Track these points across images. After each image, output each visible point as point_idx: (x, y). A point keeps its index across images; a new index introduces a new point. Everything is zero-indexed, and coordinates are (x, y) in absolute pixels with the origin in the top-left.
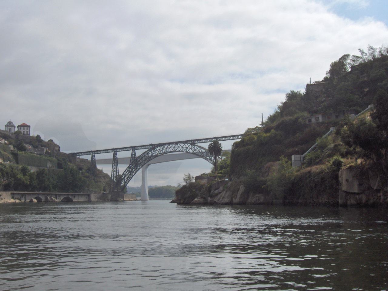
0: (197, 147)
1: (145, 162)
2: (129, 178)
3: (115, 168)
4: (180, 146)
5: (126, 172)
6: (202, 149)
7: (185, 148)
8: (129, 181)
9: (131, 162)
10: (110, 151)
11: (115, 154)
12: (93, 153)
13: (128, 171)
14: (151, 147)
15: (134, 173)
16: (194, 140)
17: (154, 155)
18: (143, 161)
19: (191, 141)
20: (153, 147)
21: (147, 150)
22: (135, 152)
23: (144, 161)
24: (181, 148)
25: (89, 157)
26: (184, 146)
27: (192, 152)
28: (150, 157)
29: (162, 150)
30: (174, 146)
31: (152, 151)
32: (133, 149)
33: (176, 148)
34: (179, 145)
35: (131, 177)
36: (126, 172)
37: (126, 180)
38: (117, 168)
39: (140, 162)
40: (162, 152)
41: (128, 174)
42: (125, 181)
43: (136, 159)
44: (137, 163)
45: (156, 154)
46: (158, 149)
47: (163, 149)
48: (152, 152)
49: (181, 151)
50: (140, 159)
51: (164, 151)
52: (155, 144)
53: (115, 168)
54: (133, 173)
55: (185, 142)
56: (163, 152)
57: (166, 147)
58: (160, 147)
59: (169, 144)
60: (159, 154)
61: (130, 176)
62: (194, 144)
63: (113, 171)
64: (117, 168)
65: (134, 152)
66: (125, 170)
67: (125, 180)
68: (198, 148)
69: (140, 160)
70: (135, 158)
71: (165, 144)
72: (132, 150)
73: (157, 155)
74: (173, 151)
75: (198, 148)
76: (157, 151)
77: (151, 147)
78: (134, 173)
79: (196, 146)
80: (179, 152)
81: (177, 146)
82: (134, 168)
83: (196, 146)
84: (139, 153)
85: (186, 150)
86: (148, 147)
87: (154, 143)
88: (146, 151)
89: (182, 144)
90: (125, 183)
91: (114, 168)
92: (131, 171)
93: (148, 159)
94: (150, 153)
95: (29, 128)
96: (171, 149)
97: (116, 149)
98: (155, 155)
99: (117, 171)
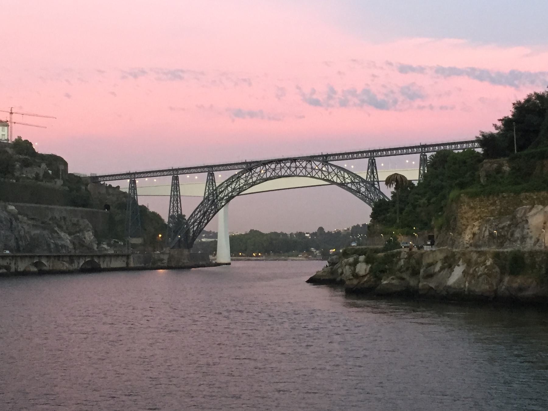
0: (334, 168)
3: (175, 205)
4: (301, 166)
5: (196, 212)
6: (342, 172)
7: (309, 170)
9: (207, 193)
10: (166, 173)
11: (176, 179)
12: (132, 176)
13: (200, 211)
14: (244, 166)
15: (211, 215)
16: (327, 156)
17: (251, 181)
18: (228, 193)
19: (322, 156)
20: (249, 167)
21: (236, 172)
22: (212, 175)
23: (232, 192)
24: (301, 169)
25: (124, 185)
26: (309, 166)
27: (323, 177)
28: (243, 186)
29: (266, 172)
30: (288, 164)
31: (247, 174)
32: (211, 170)
33: (293, 169)
34: (297, 163)
35: (206, 221)
36: (197, 214)
38: (179, 205)
40: (265, 177)
41: (199, 217)
42: (195, 229)
43: (216, 190)
44: (217, 196)
45: (254, 179)
46: (258, 169)
47: (266, 170)
48: (246, 177)
49: (301, 174)
50: (222, 189)
51: (268, 174)
52: (251, 163)
53: (175, 205)
54: (209, 214)
55: (310, 159)
56: (268, 176)
57: (273, 166)
58: (262, 167)
59: (279, 161)
60: (259, 180)
61: (204, 220)
62: (327, 162)
63: (172, 210)
64: (179, 205)
65: (211, 174)
66: (195, 211)
67: (194, 227)
68: (336, 171)
69: (222, 191)
70: (214, 188)
71: (271, 162)
72: (209, 172)
73: (254, 182)
74: (286, 174)
75: (336, 171)
76: (256, 175)
77: (244, 166)
78: (211, 215)
79: (331, 165)
80: (299, 176)
81: (293, 165)
82: (211, 206)
83: (332, 165)
84: (220, 177)
85: (311, 174)
86: (240, 166)
87: (249, 159)
89: (305, 162)
91: (173, 206)
92: (207, 211)
93: (239, 188)
94: (242, 177)
95: (6, 128)
96: (283, 171)
97: (177, 170)
98: (253, 182)
99: (179, 210)
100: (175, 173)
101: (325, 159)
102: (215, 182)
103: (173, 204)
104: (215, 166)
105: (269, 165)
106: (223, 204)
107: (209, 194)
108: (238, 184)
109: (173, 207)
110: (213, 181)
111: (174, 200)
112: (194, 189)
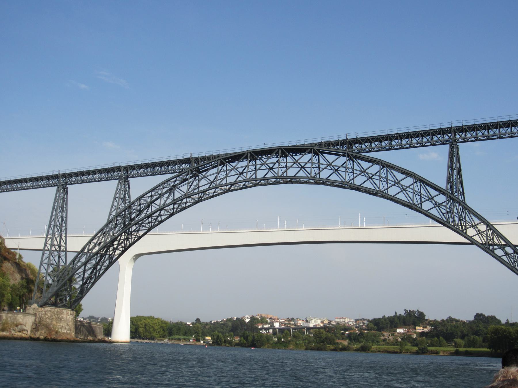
1: (160, 215)
2: (99, 267)
8: (100, 276)
15: (118, 252)
22: (126, 182)
32: (123, 173)
37: (89, 272)
38: (64, 235)
39: (143, 215)
42: (86, 275)
51: (231, 180)
52: (197, 160)
54: (114, 250)
55: (318, 149)
61: (104, 262)
63: (49, 242)
67: (85, 271)
72: (120, 179)
78: (118, 252)
88: (168, 181)
90: (84, 284)
100: (62, 181)
101: (351, 148)
102: (129, 196)
103: (53, 231)
104: (133, 167)
105: (233, 164)
106: (141, 233)
107: (118, 215)
108: (171, 198)
109: (52, 238)
110: (128, 192)
111: (55, 225)
112: (92, 208)
